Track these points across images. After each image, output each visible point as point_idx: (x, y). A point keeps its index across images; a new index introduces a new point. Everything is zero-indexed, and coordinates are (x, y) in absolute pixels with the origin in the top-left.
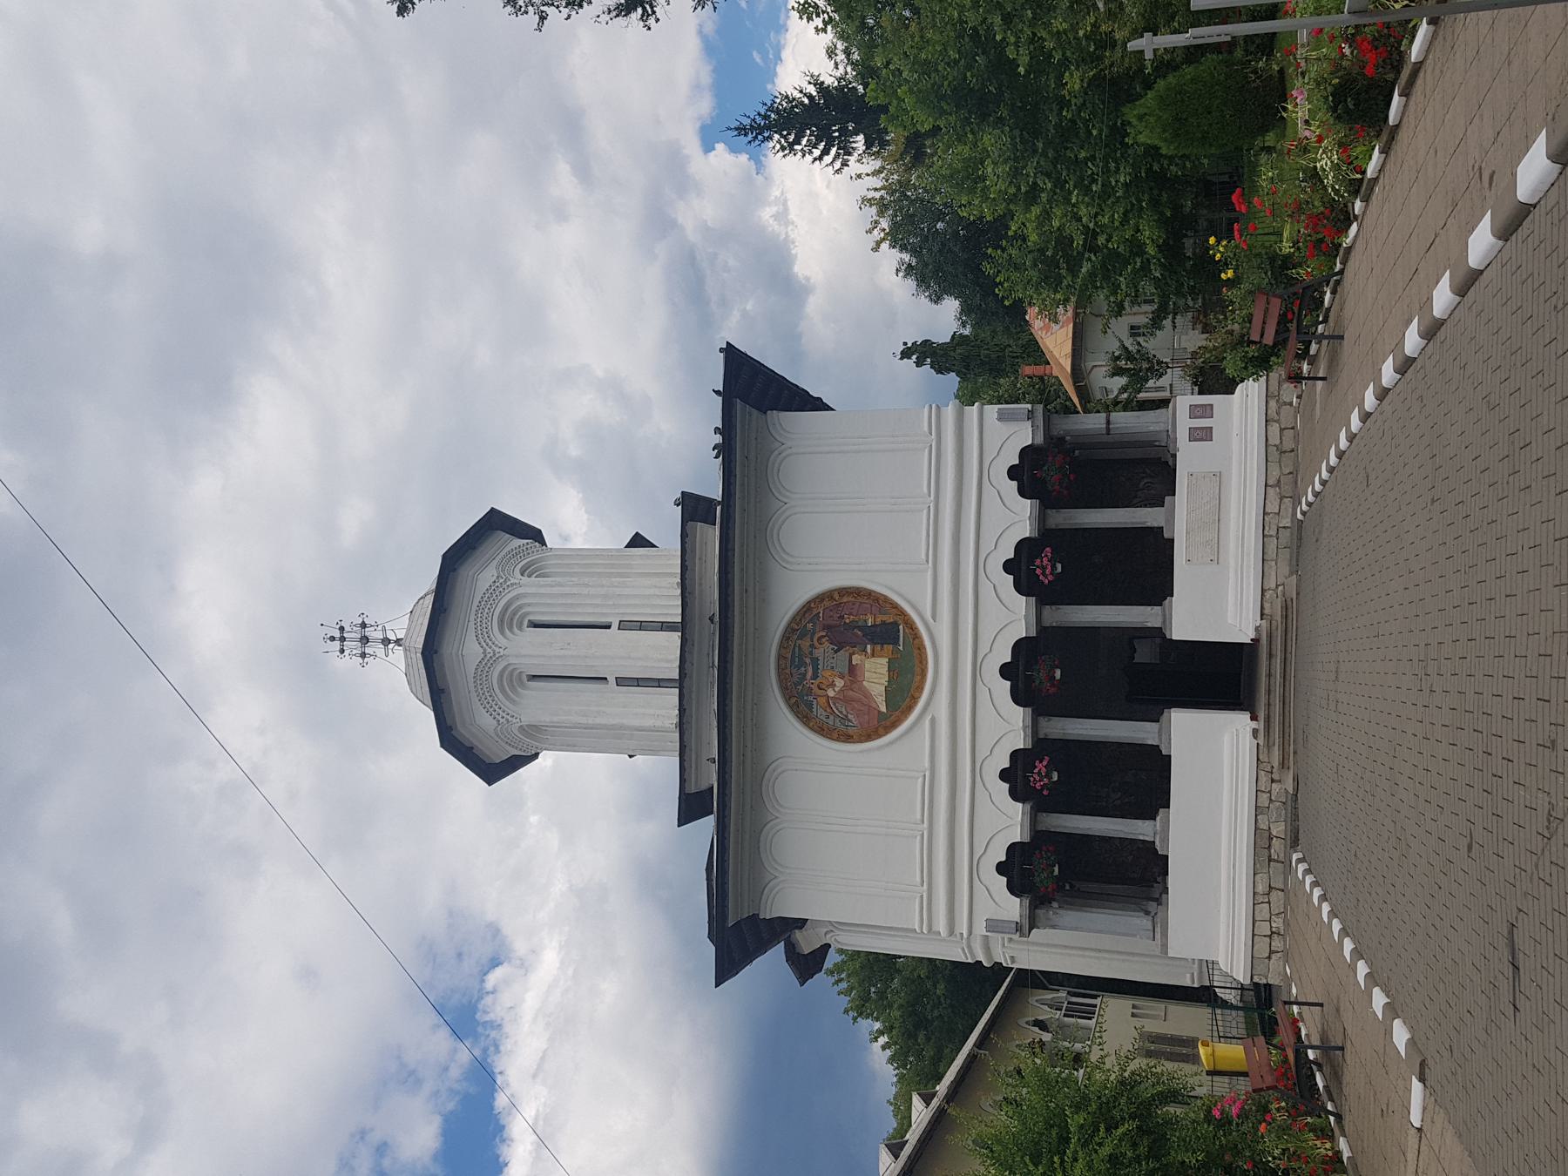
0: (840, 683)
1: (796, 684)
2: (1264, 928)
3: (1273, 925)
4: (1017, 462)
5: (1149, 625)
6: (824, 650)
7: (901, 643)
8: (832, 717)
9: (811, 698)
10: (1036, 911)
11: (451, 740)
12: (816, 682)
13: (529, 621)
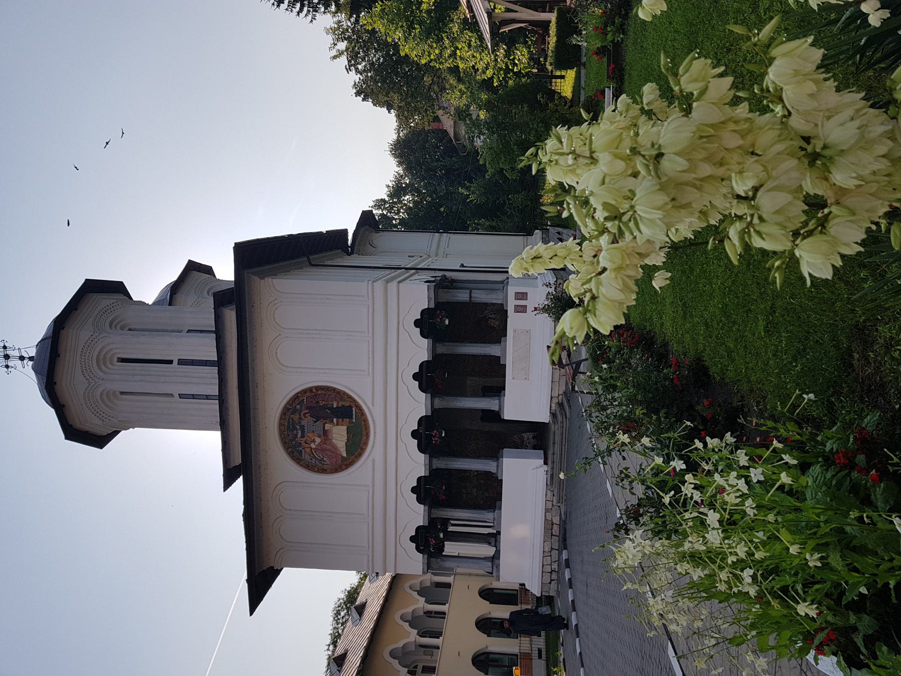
0: (318, 440)
1: (291, 441)
2: (548, 569)
3: (553, 567)
4: (419, 318)
5: (492, 409)
6: (307, 421)
7: (354, 418)
8: (314, 459)
9: (301, 449)
10: (431, 559)
11: (73, 432)
12: (304, 439)
13: (118, 358)
